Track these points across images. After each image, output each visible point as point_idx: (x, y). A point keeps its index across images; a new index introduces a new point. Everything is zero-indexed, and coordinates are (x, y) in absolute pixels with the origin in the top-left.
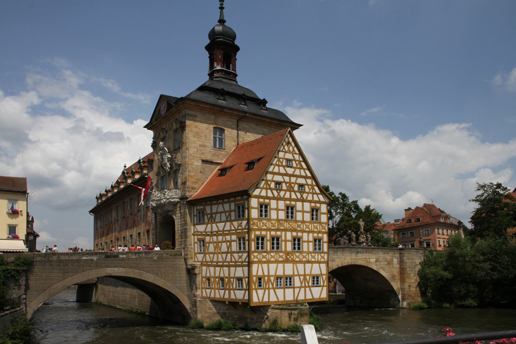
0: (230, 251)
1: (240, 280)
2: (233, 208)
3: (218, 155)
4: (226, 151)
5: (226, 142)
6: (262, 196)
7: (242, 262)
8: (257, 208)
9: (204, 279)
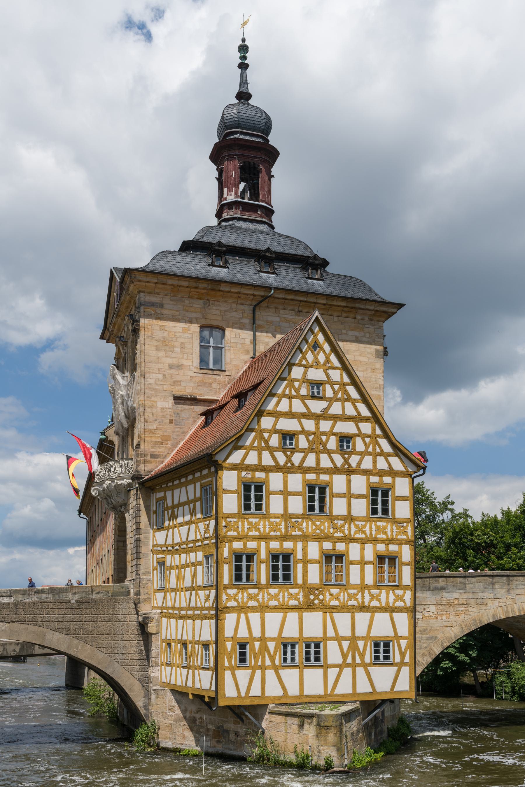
0: (194, 585)
1: (206, 646)
2: (198, 495)
3: (210, 384)
4: (227, 373)
5: (228, 355)
6: (248, 465)
7: (209, 609)
8: (237, 492)
9: (164, 644)
